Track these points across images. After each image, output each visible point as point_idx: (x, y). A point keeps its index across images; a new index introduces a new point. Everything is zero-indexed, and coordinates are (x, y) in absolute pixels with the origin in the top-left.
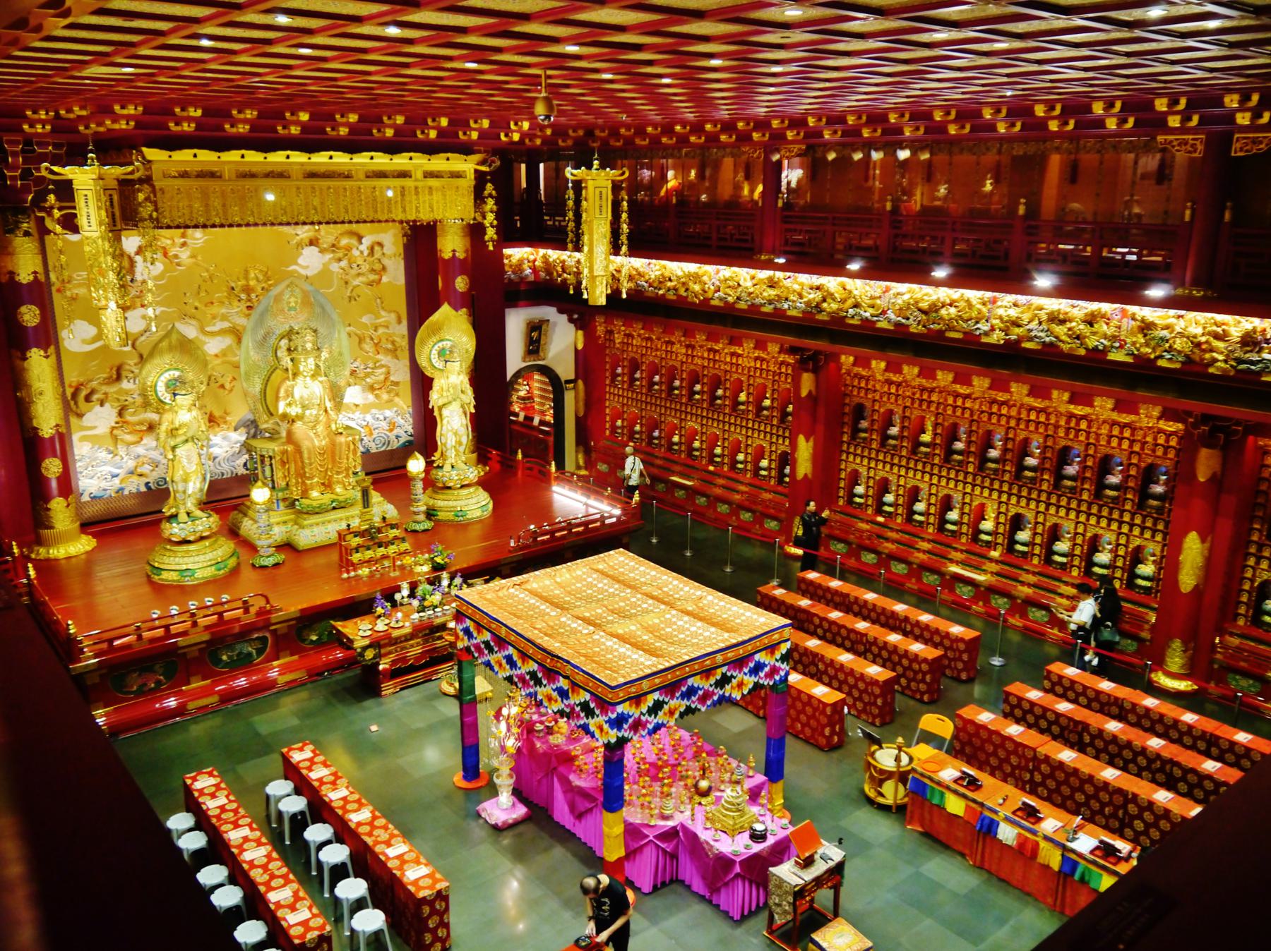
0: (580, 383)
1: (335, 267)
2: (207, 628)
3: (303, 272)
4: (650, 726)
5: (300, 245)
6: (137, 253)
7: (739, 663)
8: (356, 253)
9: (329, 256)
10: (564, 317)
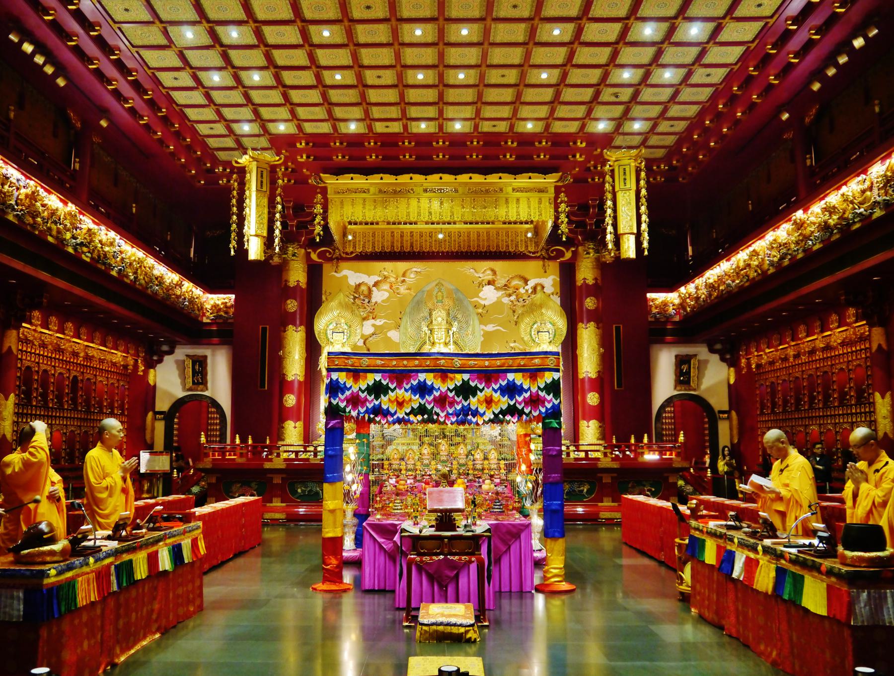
0: (734, 413)
1: (506, 300)
2: (285, 460)
3: (483, 303)
4: (370, 406)
5: (481, 285)
6: (374, 286)
7: (488, 376)
8: (522, 291)
9: (500, 293)
10: (715, 358)
